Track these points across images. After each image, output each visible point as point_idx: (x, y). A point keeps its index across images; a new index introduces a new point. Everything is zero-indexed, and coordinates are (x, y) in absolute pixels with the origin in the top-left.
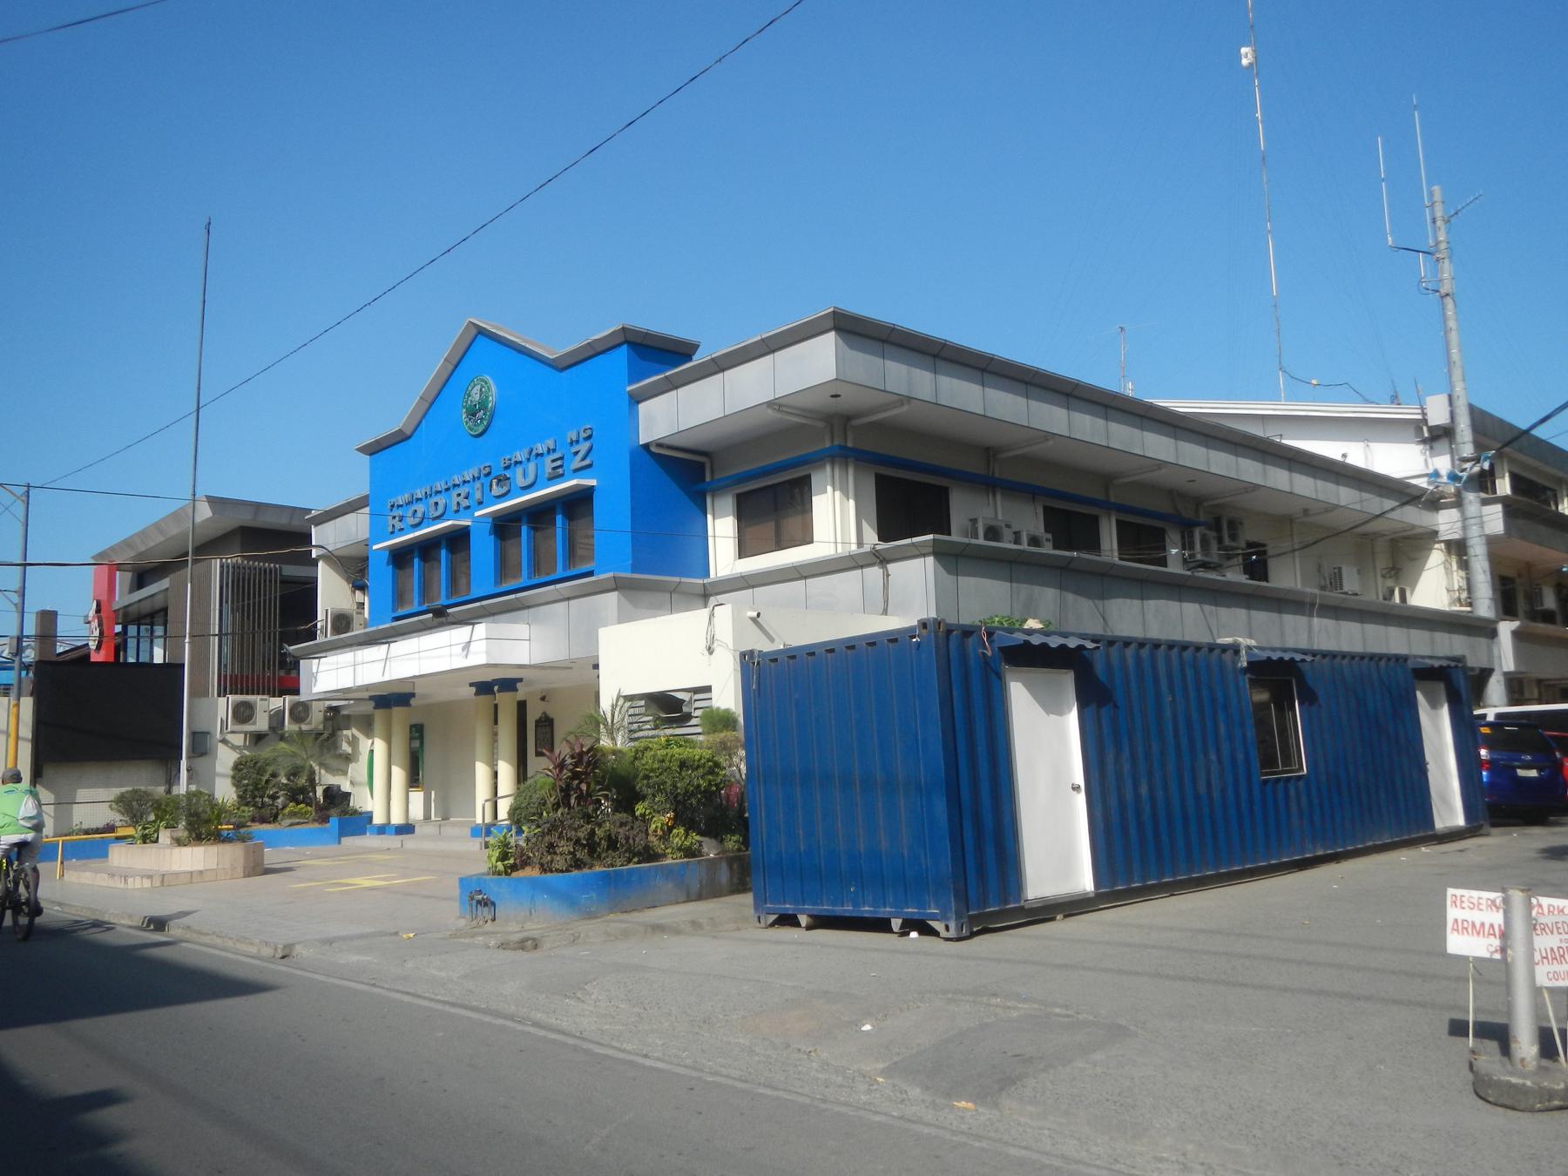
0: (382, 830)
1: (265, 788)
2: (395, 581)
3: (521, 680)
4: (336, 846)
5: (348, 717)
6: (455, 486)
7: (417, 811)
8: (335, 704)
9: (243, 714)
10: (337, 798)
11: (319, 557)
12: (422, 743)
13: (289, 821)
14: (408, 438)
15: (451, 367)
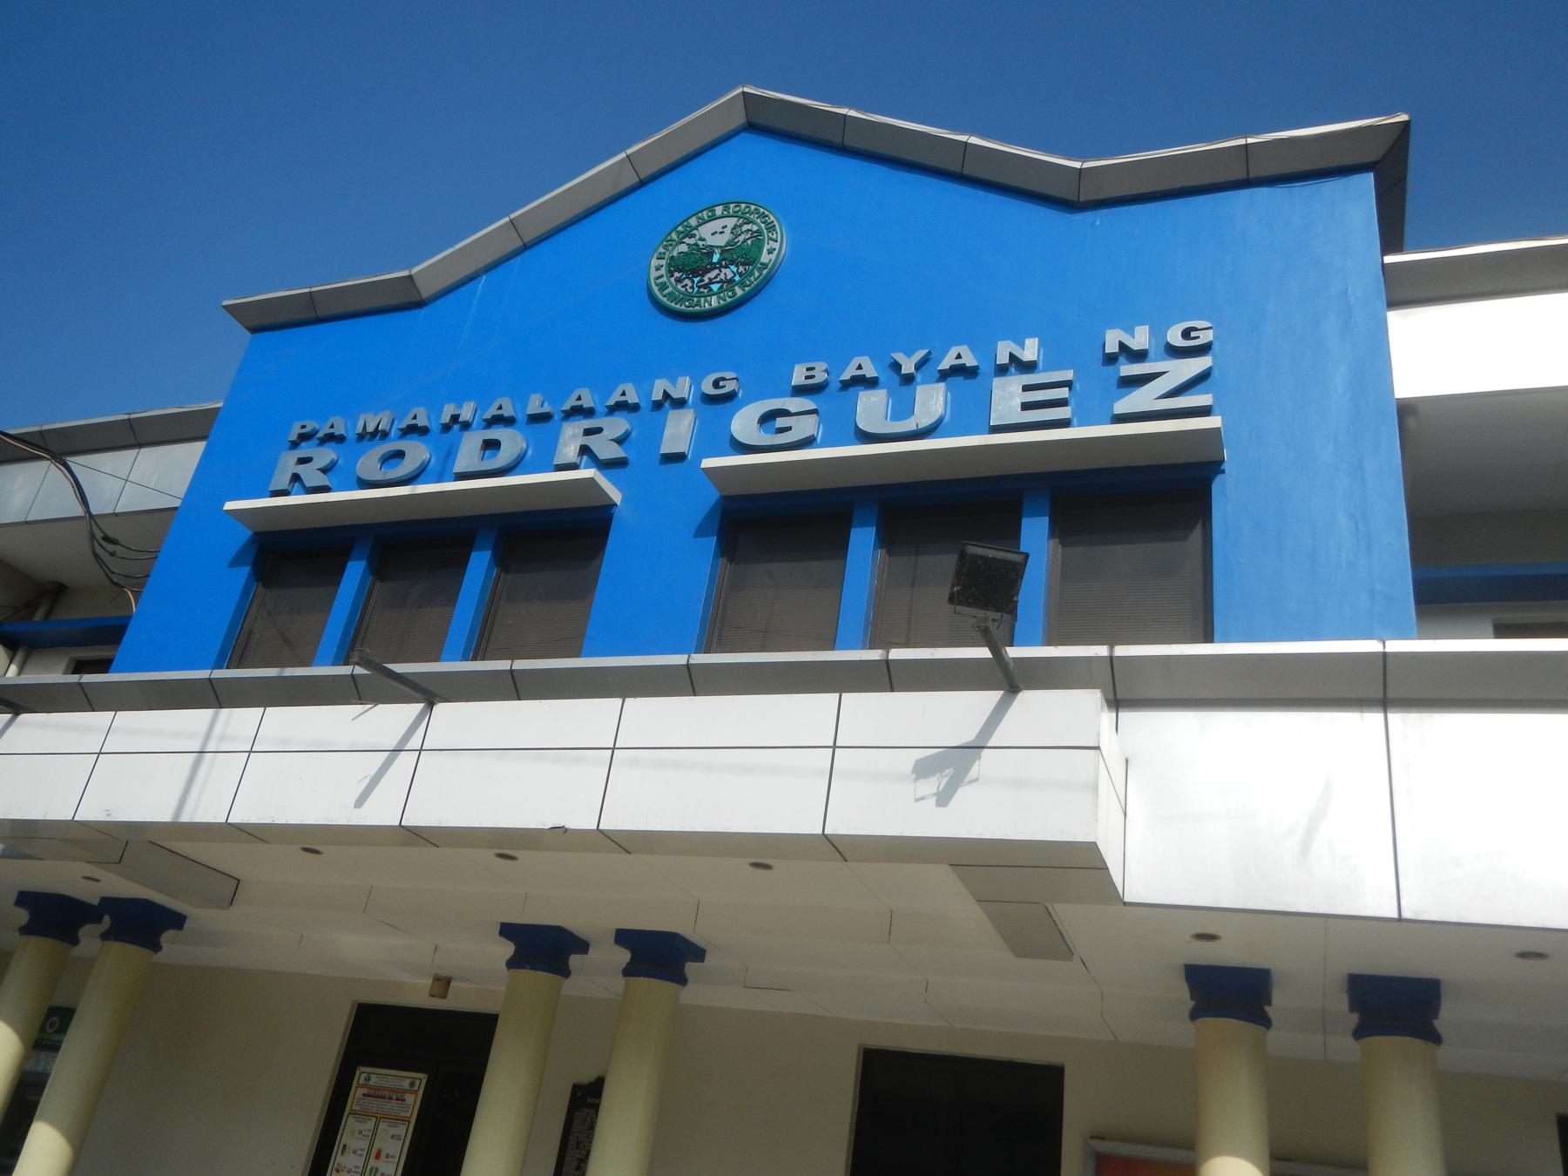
2: (243, 610)
3: (698, 954)
6: (577, 412)
14: (420, 304)
15: (631, 179)
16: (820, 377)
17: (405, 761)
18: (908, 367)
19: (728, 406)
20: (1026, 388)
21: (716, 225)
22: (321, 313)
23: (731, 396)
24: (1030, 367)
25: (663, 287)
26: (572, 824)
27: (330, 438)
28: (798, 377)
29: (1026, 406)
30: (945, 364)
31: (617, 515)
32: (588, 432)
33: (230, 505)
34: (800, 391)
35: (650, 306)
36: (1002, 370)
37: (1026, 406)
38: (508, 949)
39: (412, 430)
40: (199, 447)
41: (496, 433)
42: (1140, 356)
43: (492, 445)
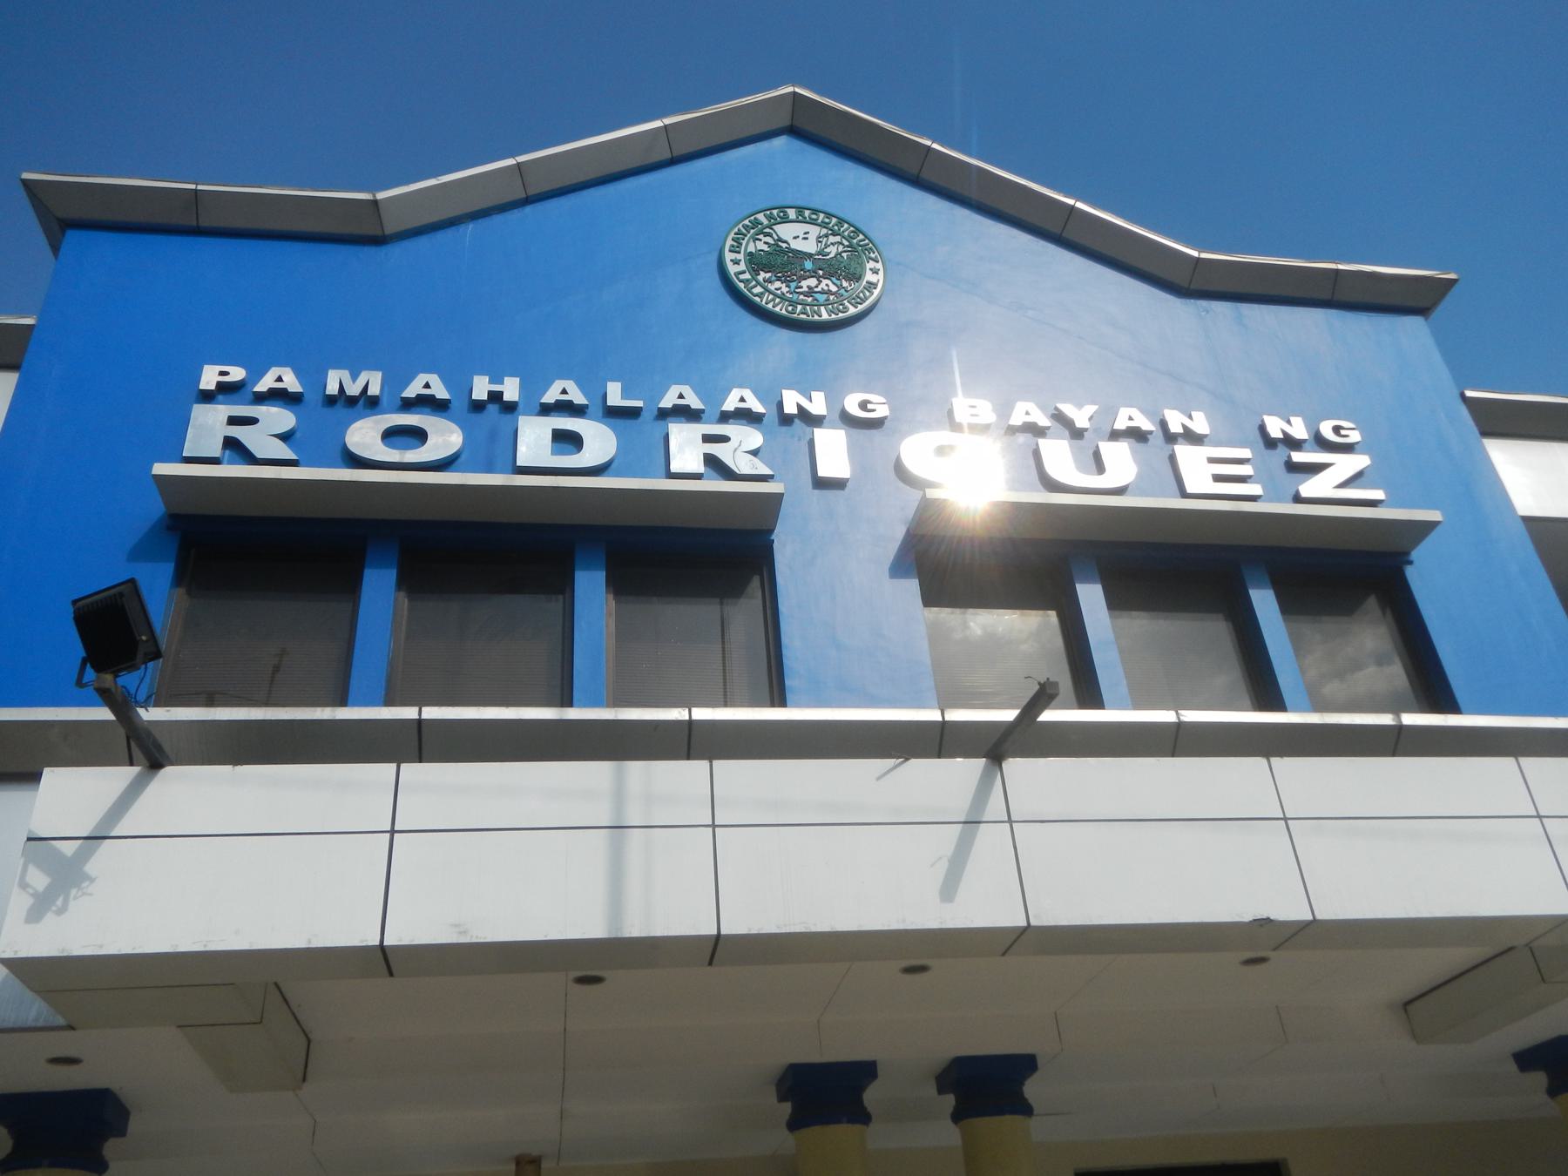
14: (379, 240)
17: (991, 838)
18: (1081, 417)
20: (1212, 460)
21: (799, 229)
22: (205, 222)
23: (877, 424)
29: (1218, 478)
33: (160, 469)
35: (727, 300)
37: (1218, 478)
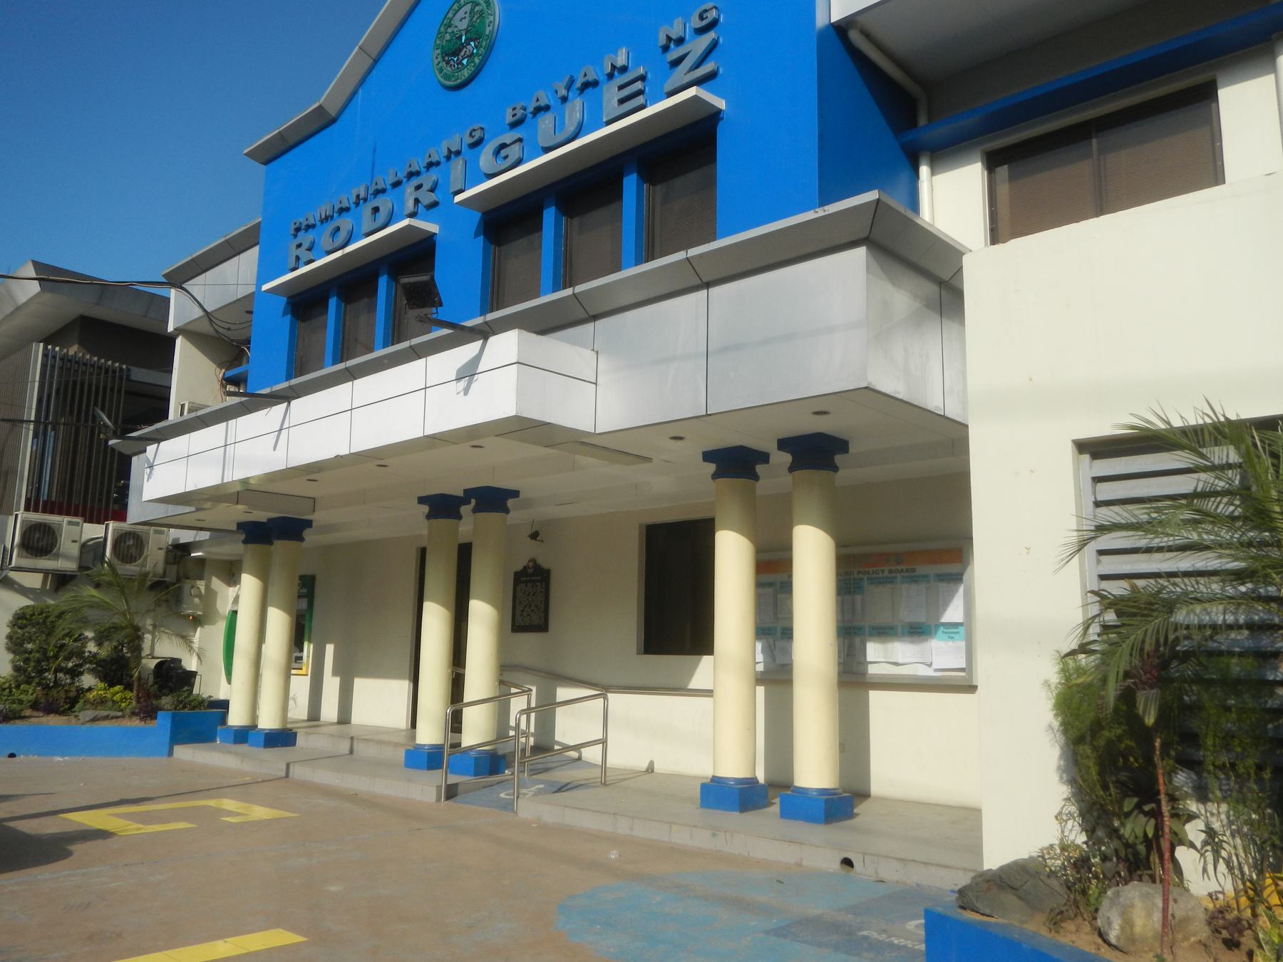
0: (243, 735)
1: (56, 657)
3: (515, 494)
4: (165, 759)
5: (201, 561)
6: (411, 175)
7: (299, 710)
8: (186, 536)
9: (39, 542)
10: (174, 678)
11: (179, 331)
12: (311, 605)
13: (90, 714)
14: (334, 121)
16: (520, 113)
19: (478, 148)
20: (621, 88)
21: (461, 14)
22: (291, 142)
24: (624, 69)
25: (441, 70)
26: (342, 454)
27: (309, 227)
28: (509, 119)
29: (622, 101)
30: (578, 84)
31: (438, 240)
32: (418, 187)
33: (265, 287)
34: (515, 125)
36: (610, 76)
37: (622, 101)
38: (426, 509)
39: (343, 210)
40: (257, 249)
41: (379, 201)
42: (680, 41)
43: (376, 210)
